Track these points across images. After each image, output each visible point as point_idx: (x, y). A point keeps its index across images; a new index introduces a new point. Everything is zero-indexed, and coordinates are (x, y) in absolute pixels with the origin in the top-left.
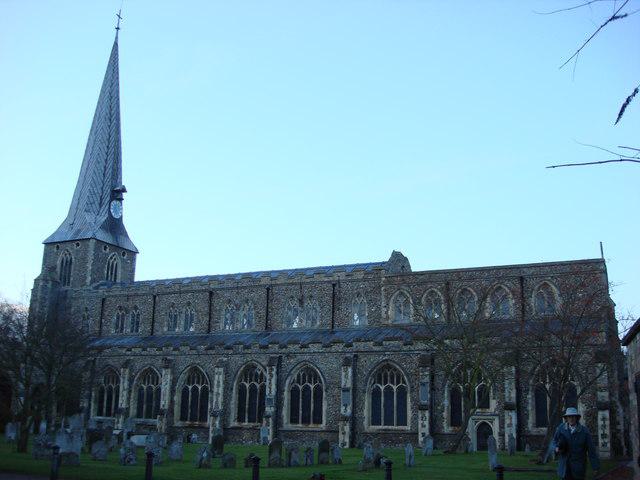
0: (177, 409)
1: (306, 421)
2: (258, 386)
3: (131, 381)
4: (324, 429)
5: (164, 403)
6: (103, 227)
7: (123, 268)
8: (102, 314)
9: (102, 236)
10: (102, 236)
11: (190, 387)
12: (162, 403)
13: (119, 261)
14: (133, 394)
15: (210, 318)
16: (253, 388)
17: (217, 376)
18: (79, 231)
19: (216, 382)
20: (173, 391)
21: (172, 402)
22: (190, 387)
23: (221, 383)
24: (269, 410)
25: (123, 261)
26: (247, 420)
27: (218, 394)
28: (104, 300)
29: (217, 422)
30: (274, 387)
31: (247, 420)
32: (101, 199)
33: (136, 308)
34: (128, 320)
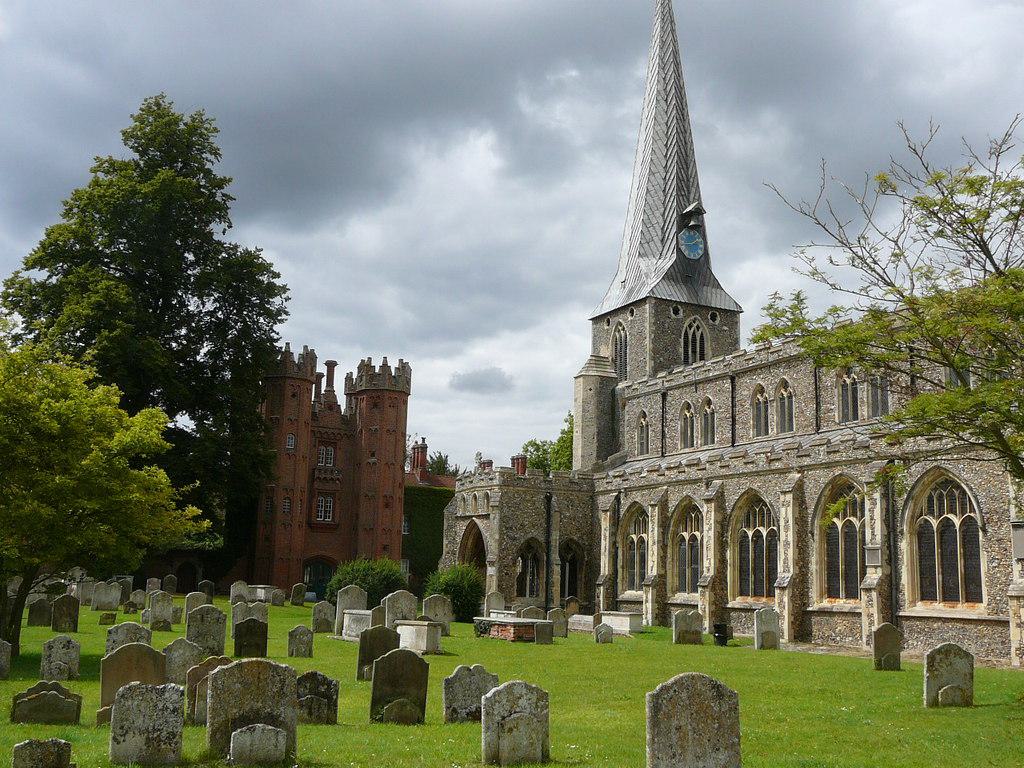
0: (731, 574)
1: (950, 596)
2: (857, 524)
3: (664, 525)
4: (985, 616)
5: (709, 563)
6: (669, 276)
7: (715, 339)
8: (663, 419)
9: (677, 294)
10: (677, 294)
11: (750, 534)
12: (706, 563)
13: (706, 330)
14: (669, 551)
15: (818, 404)
16: (849, 525)
17: (783, 510)
18: (631, 291)
19: (782, 523)
20: (721, 545)
21: (722, 562)
22: (750, 534)
23: (791, 522)
24: (873, 576)
25: (713, 328)
26: (842, 593)
27: (787, 543)
28: (664, 396)
29: (786, 599)
30: (878, 525)
31: (842, 593)
32: (664, 233)
33: (709, 402)
34: (698, 425)
